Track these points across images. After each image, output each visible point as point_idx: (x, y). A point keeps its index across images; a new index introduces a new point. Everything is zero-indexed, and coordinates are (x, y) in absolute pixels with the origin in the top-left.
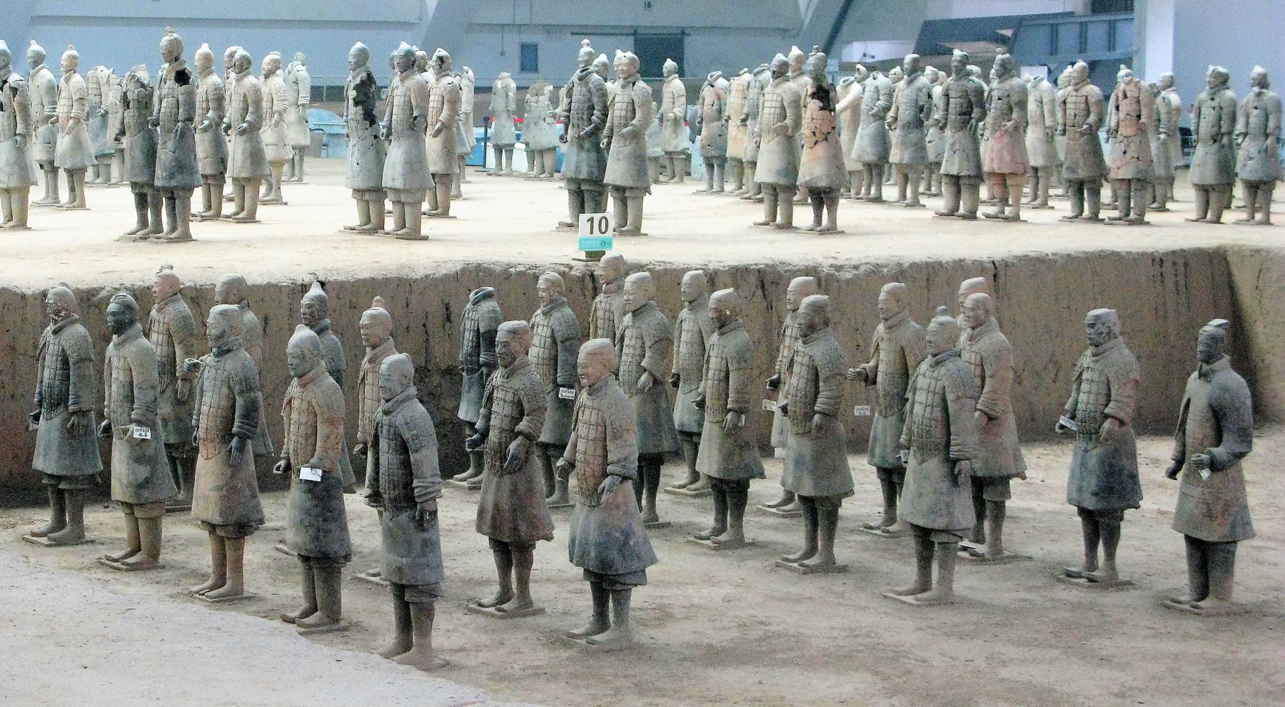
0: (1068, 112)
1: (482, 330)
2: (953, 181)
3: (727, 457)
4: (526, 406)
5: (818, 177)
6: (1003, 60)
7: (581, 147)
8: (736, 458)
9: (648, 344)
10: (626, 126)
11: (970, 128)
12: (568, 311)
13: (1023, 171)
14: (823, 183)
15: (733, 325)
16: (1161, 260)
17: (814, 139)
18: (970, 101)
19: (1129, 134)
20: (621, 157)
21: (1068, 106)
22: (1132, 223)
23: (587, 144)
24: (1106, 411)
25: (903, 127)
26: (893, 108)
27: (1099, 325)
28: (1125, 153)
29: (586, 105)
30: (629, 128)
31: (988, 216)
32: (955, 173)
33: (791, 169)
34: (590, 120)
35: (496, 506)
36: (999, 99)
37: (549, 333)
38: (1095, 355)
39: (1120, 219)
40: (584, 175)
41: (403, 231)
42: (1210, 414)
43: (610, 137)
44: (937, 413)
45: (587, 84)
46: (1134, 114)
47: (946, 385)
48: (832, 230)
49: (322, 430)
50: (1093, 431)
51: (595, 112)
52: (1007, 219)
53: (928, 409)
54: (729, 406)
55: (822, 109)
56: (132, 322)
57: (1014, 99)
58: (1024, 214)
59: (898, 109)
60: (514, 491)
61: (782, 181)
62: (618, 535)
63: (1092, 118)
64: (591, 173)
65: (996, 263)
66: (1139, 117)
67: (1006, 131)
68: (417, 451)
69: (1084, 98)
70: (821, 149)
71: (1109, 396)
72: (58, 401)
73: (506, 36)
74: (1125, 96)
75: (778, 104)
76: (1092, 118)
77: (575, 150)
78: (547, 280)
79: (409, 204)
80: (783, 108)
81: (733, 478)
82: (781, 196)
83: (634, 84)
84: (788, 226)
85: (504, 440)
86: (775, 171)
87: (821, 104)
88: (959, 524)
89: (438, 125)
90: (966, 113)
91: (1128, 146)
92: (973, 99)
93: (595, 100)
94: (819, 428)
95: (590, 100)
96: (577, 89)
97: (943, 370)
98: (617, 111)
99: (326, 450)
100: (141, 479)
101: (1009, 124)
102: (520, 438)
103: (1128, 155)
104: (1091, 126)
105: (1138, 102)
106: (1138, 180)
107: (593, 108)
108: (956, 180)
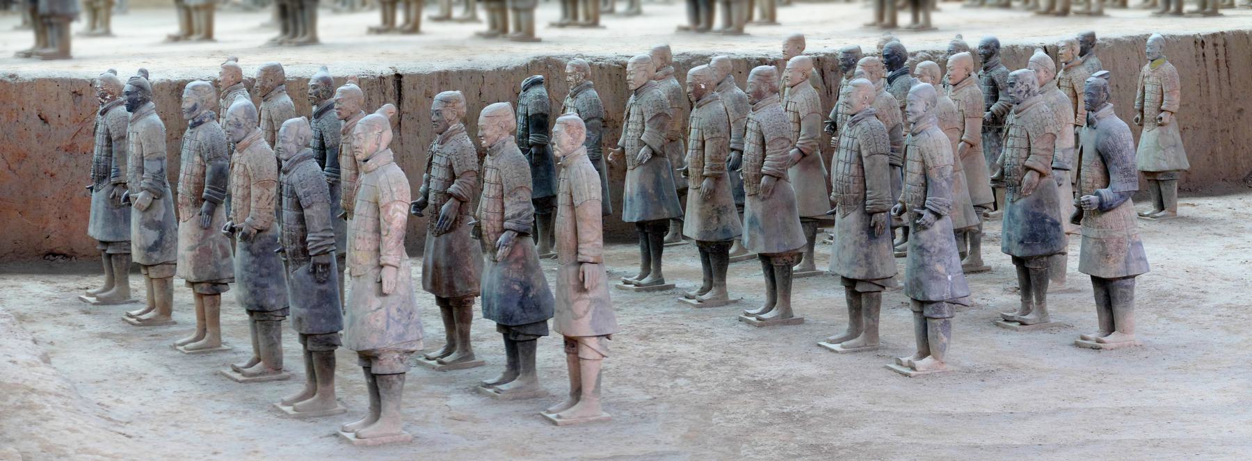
1: (529, 115)
3: (706, 221)
4: (456, 170)
8: (715, 221)
9: (647, 119)
12: (593, 93)
15: (708, 98)
35: (436, 266)
44: (854, 169)
47: (861, 142)
48: (927, 27)
49: (255, 191)
53: (847, 166)
54: (705, 173)
56: (145, 101)
60: (449, 250)
62: (517, 287)
68: (309, 207)
72: (103, 175)
78: (573, 66)
81: (712, 239)
84: (893, 25)
85: (438, 202)
88: (878, 274)
94: (766, 188)
97: (858, 129)
99: (259, 210)
100: (151, 243)
102: (451, 199)
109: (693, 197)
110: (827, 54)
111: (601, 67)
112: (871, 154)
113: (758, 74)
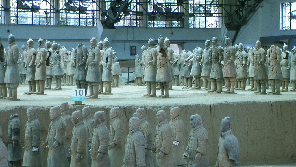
0: (254, 57)
1: (12, 129)
2: (214, 80)
5: (162, 79)
6: (227, 40)
7: (79, 69)
9: (57, 131)
10: (92, 62)
11: (219, 62)
13: (235, 77)
14: (163, 81)
16: (272, 105)
17: (160, 66)
18: (218, 54)
19: (273, 64)
20: (91, 72)
21: (255, 55)
22: (275, 94)
23: (81, 69)
24: (197, 150)
25: (205, 64)
26: (202, 58)
27: (194, 120)
28: (272, 70)
29: (81, 55)
30: (93, 62)
31: (224, 92)
32: (214, 78)
33: (154, 76)
34: (82, 60)
36: (226, 53)
37: (30, 129)
38: (194, 131)
39: (271, 93)
40: (80, 78)
41: (11, 97)
42: (225, 150)
43: (88, 66)
44: (132, 151)
45: (81, 48)
46: (275, 57)
48: (167, 96)
50: (193, 157)
51: (84, 58)
52: (229, 93)
53: (129, 149)
54: (77, 151)
55: (163, 56)
57: (231, 52)
58: (236, 92)
59: (204, 58)
61: (152, 81)
63: (262, 59)
64: (82, 78)
65: (211, 106)
66: (276, 58)
67: (228, 63)
69: (259, 53)
70: (162, 70)
71: (198, 144)
73: (125, 44)
74: (272, 52)
75: (150, 55)
76: (262, 59)
77: (78, 70)
78: (29, 110)
79: (13, 88)
80: (151, 56)
82: (152, 86)
83: (95, 48)
84: (154, 95)
86: (149, 77)
87: (162, 55)
89: (39, 64)
90: (217, 58)
91: (273, 68)
92: (219, 53)
93: (84, 53)
94: (99, 157)
95: (82, 54)
96: (78, 50)
97: (133, 135)
98: (90, 57)
101: (229, 61)
103: (273, 71)
104: (261, 62)
105: (276, 54)
106: (277, 79)
107: (83, 56)
108: (215, 80)
109: (73, 160)
110: (127, 106)
111: (41, 111)
112: (138, 145)
113: (98, 114)
